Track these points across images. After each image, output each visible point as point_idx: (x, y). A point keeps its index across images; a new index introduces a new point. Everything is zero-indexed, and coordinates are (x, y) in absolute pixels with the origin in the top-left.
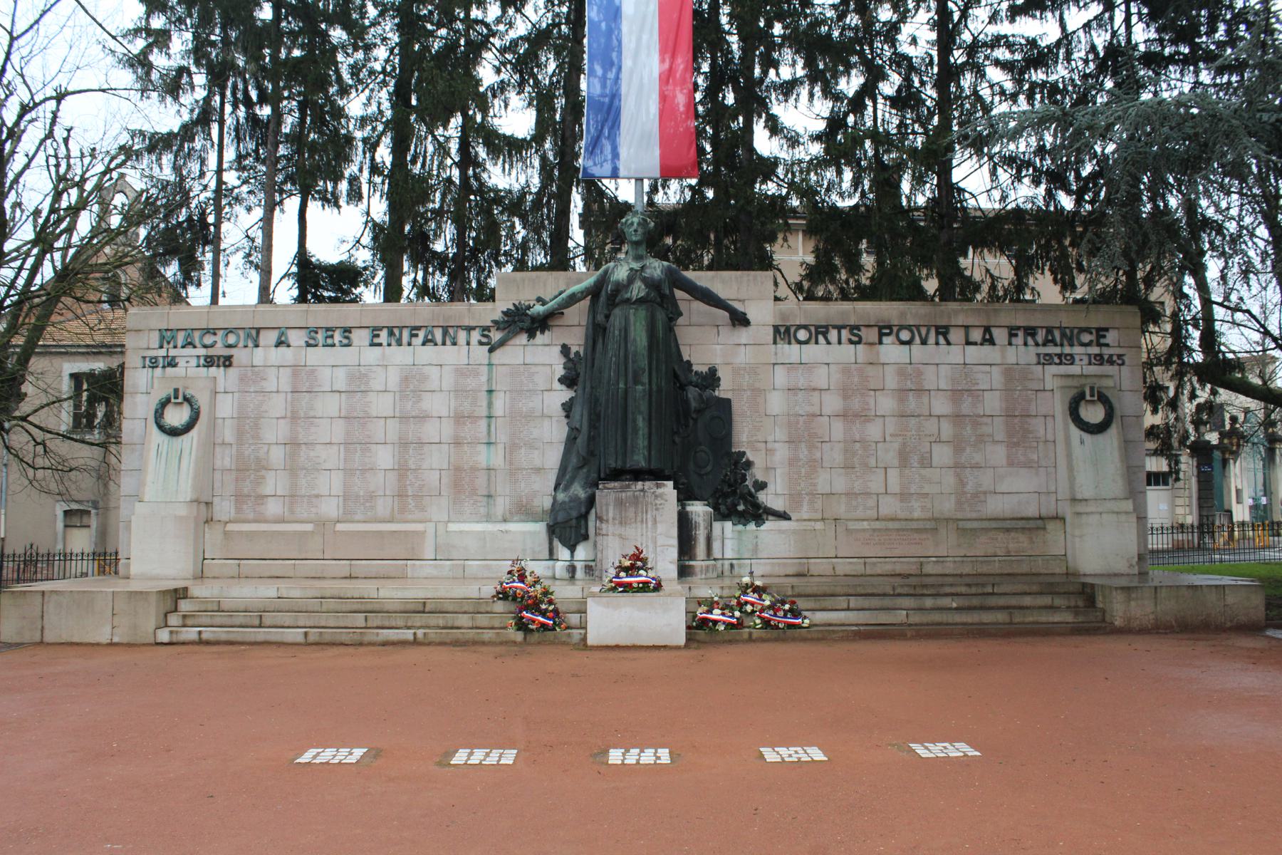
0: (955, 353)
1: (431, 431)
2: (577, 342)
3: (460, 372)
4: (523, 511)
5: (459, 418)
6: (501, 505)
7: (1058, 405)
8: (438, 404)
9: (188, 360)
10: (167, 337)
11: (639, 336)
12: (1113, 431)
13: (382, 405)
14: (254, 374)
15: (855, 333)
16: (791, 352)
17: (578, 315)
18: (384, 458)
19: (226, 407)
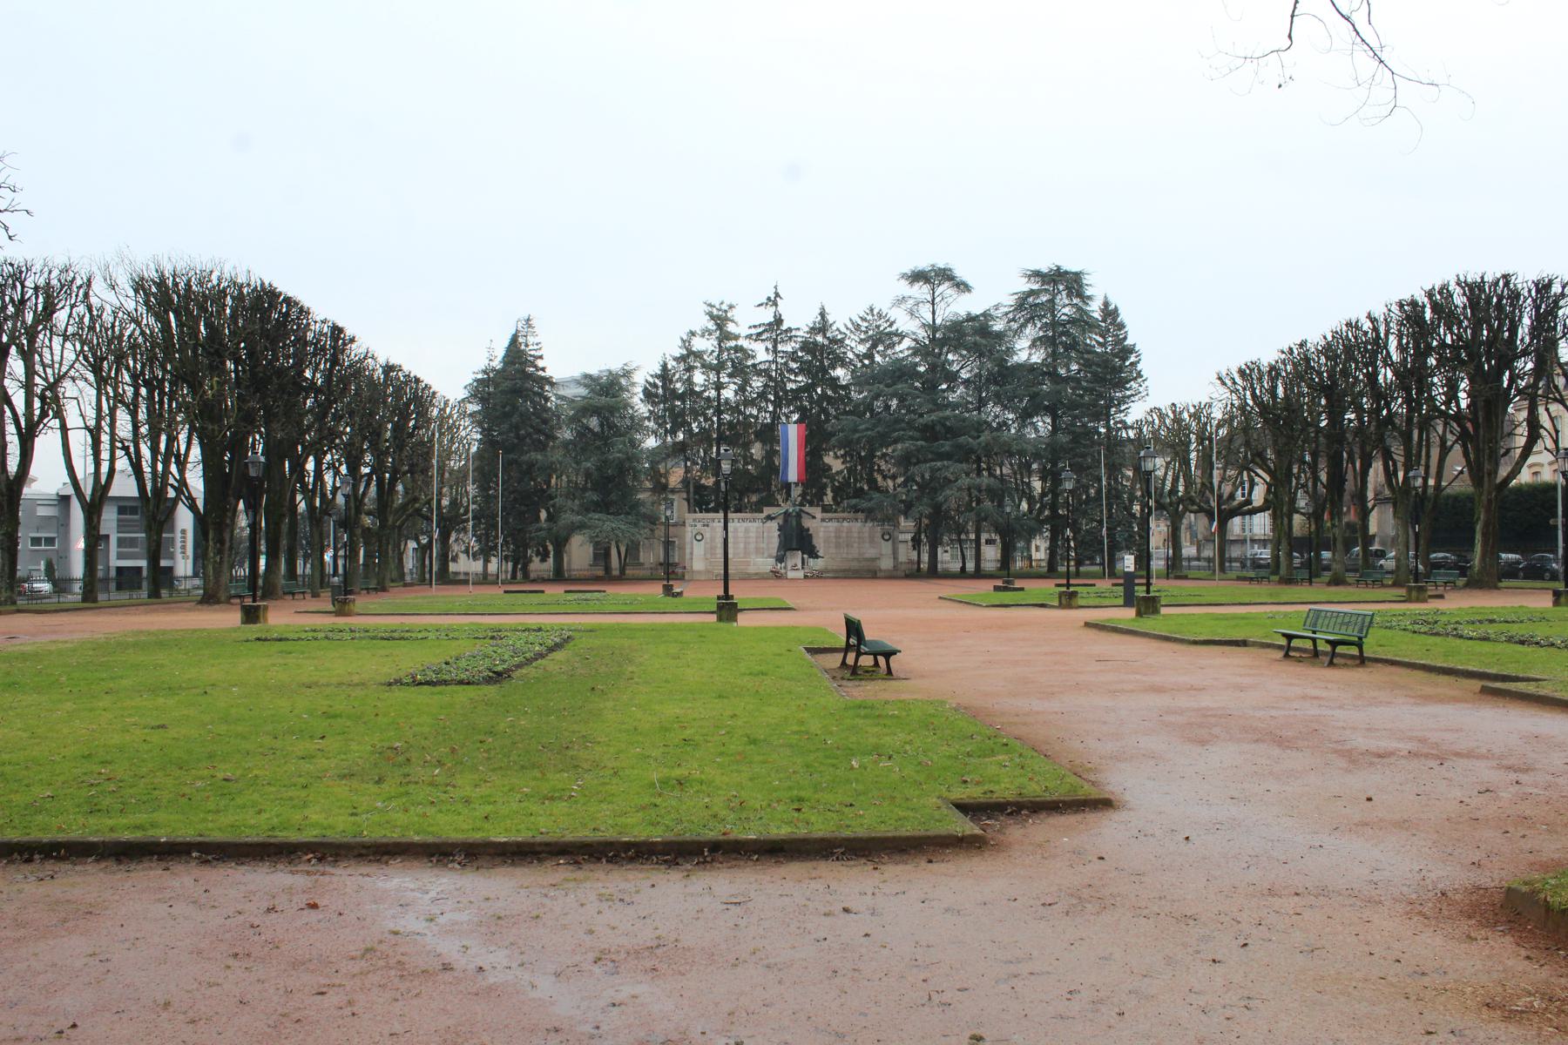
0: (859, 524)
1: (751, 540)
2: (781, 523)
3: (757, 528)
4: (770, 556)
5: (757, 538)
6: (766, 555)
7: (879, 535)
8: (752, 535)
9: (699, 525)
10: (694, 520)
11: (794, 523)
12: (890, 542)
13: (741, 535)
14: (713, 529)
15: (838, 520)
16: (825, 524)
17: (782, 516)
18: (742, 545)
19: (707, 535)
